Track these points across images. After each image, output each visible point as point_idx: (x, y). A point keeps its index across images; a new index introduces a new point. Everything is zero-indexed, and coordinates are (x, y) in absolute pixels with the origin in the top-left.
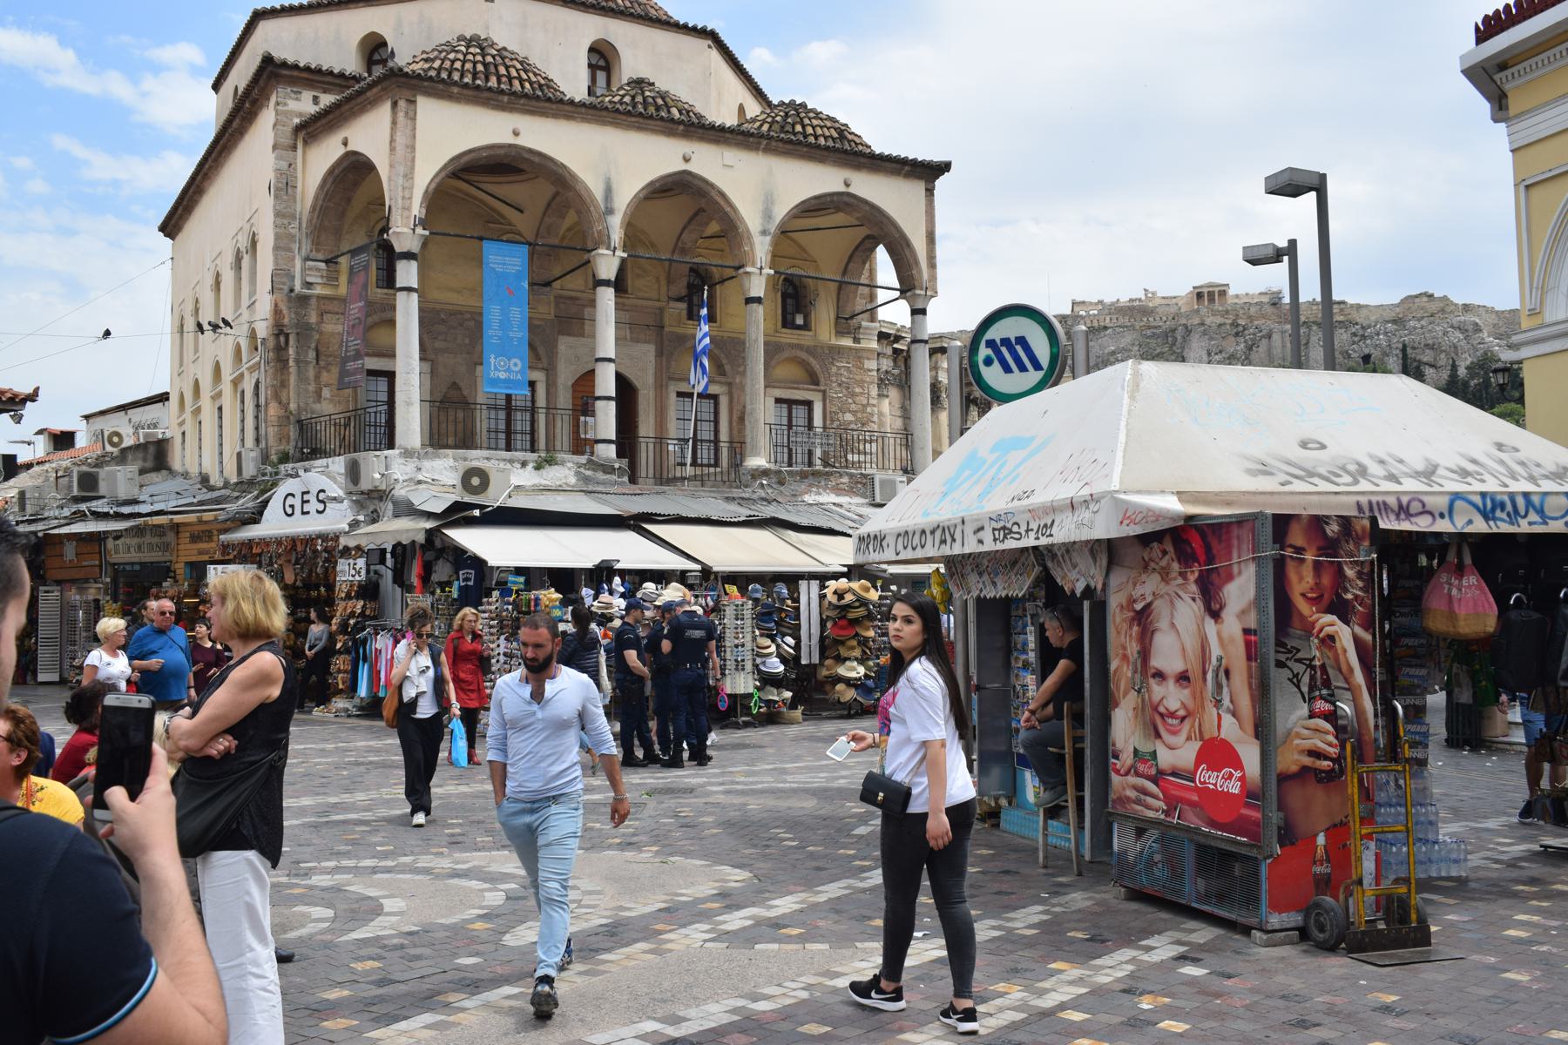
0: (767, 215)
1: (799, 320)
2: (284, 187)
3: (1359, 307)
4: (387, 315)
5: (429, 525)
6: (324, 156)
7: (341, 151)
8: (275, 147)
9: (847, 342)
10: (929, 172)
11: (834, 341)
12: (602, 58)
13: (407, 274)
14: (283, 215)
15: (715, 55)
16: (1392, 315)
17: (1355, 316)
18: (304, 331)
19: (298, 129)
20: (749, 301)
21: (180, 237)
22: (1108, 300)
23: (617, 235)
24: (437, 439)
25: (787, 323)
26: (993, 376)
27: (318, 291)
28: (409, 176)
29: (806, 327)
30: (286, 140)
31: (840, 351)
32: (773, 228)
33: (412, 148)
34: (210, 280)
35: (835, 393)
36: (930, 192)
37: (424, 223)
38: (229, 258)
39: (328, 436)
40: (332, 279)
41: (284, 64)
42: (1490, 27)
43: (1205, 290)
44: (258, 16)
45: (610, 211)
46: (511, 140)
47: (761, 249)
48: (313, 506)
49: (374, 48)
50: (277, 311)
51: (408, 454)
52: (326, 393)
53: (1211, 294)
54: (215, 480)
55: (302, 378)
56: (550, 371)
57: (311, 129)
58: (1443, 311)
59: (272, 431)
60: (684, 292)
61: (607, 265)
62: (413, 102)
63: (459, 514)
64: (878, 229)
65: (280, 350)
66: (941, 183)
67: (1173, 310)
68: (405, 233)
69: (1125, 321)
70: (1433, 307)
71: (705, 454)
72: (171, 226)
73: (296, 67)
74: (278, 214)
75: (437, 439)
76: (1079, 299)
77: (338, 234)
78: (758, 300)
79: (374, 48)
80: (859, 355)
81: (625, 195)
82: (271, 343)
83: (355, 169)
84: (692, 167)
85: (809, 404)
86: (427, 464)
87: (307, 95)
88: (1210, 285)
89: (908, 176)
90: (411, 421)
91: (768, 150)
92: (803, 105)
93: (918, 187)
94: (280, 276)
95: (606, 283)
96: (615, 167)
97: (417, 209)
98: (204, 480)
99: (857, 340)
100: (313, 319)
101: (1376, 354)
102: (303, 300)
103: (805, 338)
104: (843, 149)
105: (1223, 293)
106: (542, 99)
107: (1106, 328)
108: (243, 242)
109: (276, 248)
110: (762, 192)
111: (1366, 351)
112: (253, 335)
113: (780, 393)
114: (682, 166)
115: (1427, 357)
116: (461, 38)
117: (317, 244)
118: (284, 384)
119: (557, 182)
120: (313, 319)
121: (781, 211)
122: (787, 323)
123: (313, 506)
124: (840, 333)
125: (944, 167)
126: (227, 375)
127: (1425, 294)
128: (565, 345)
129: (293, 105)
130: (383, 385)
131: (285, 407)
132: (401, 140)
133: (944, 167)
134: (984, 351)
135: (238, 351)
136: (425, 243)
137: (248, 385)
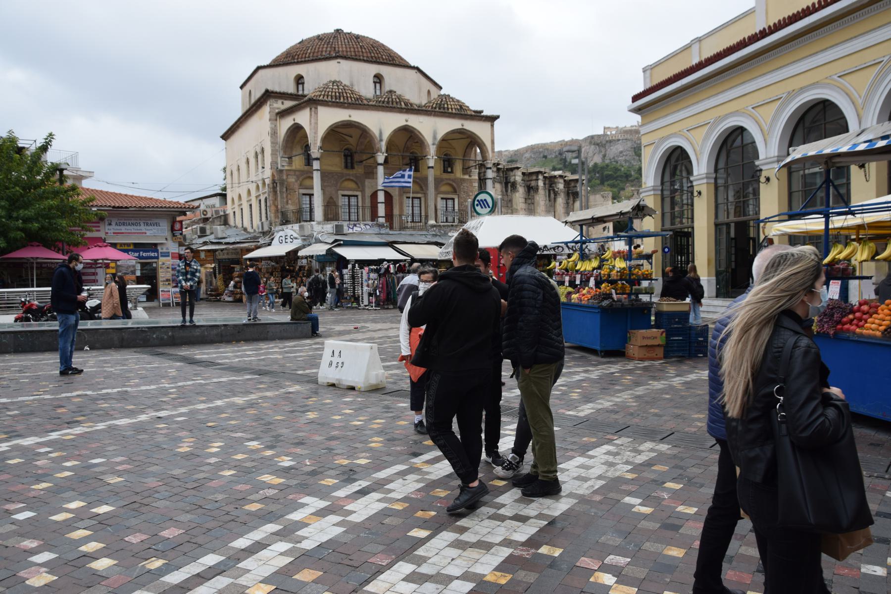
0: (435, 138)
1: (449, 170)
2: (274, 133)
4: (309, 175)
5: (328, 247)
6: (286, 124)
7: (293, 122)
8: (270, 120)
9: (467, 177)
10: (492, 119)
11: (462, 177)
12: (378, 79)
13: (316, 165)
14: (274, 143)
15: (419, 74)
18: (282, 183)
19: (278, 114)
20: (429, 167)
21: (229, 141)
22: (621, 126)
23: (384, 148)
24: (327, 218)
25: (445, 171)
26: (478, 209)
27: (286, 168)
28: (316, 133)
29: (452, 172)
30: (274, 117)
31: (464, 180)
32: (437, 142)
33: (316, 123)
34: (245, 160)
35: (463, 195)
36: (492, 126)
37: (321, 148)
38: (253, 154)
39: (291, 216)
40: (290, 163)
41: (272, 92)
42: (635, 98)
44: (259, 68)
45: (381, 140)
46: (346, 118)
47: (432, 150)
48: (289, 240)
49: (299, 80)
50: (273, 175)
51: (319, 223)
52: (290, 202)
54: (250, 229)
55: (282, 198)
56: (363, 191)
57: (283, 114)
59: (273, 215)
60: (408, 162)
61: (381, 158)
62: (316, 108)
63: (338, 243)
64: (473, 141)
65: (274, 188)
66: (496, 123)
68: (315, 152)
69: (628, 136)
71: (417, 219)
72: (226, 136)
73: (276, 93)
74: (272, 143)
75: (327, 218)
77: (292, 149)
78: (432, 167)
79: (299, 80)
80: (471, 181)
81: (386, 136)
82: (271, 186)
83: (297, 129)
84: (409, 123)
85: (453, 199)
86: (325, 226)
87: (280, 101)
89: (484, 121)
90: (319, 213)
91: (435, 115)
92: (449, 96)
93: (488, 125)
94: (274, 164)
95: (381, 164)
96: (383, 125)
97: (319, 144)
98: (245, 230)
99: (470, 176)
100: (285, 177)
102: (281, 171)
103: (452, 176)
104: (462, 112)
106: (359, 103)
107: (619, 140)
108: (259, 150)
109: (272, 154)
110: (432, 129)
112: (264, 183)
113: (442, 196)
114: (404, 123)
116: (330, 82)
117: (285, 152)
118: (276, 199)
119: (363, 131)
120: (285, 177)
121: (439, 136)
122: (445, 171)
123: (289, 240)
124: (464, 174)
125: (498, 117)
126: (254, 193)
128: (368, 182)
129: (275, 105)
130: (308, 198)
131: (277, 207)
132: (313, 121)
133: (498, 117)
134: (476, 203)
135: (258, 187)
136: (321, 156)
137: (263, 198)
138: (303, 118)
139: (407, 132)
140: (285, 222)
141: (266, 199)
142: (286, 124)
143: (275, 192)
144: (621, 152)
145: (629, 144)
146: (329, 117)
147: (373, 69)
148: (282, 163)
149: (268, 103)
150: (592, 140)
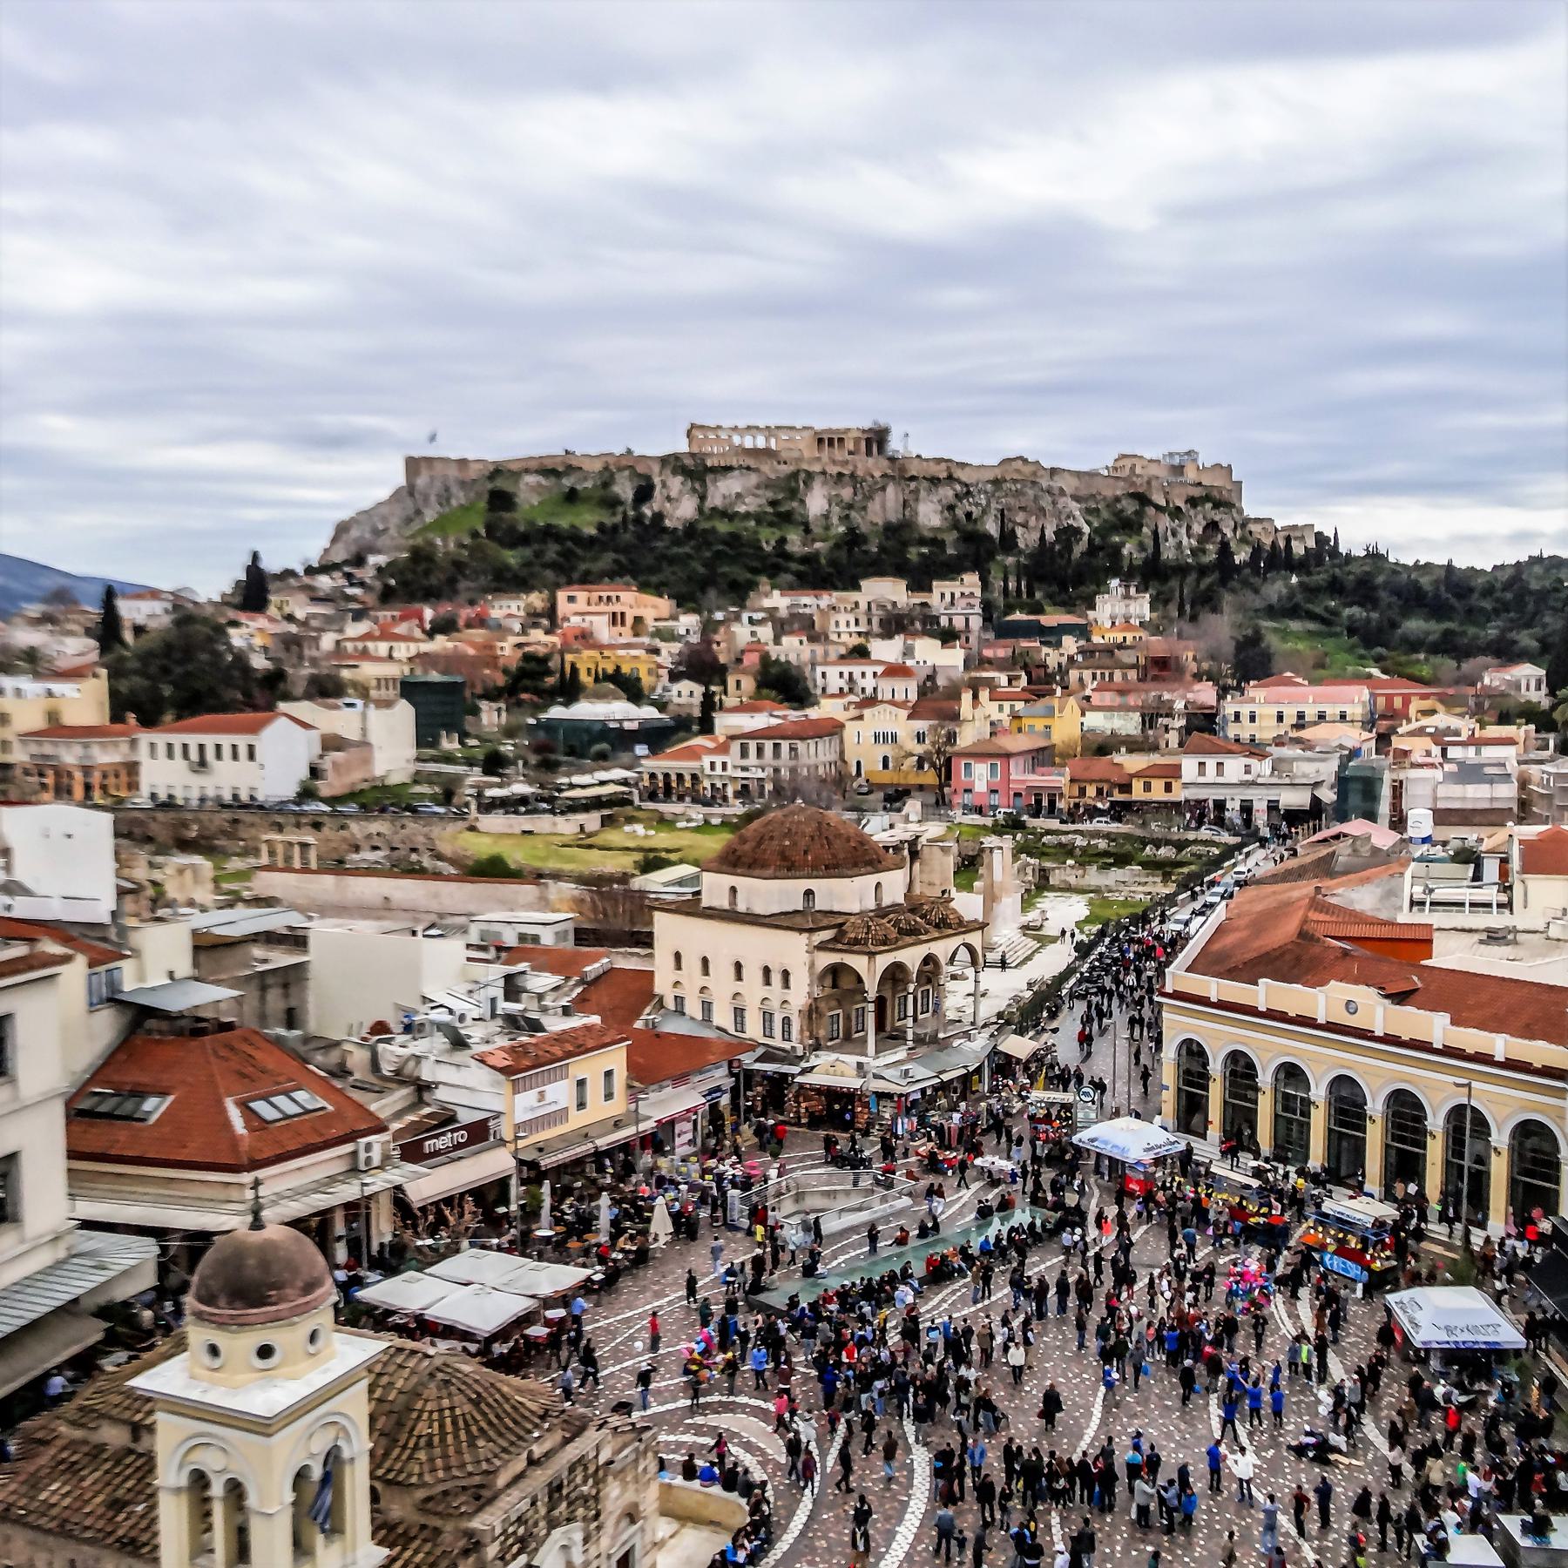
2: (812, 966)
3: (963, 465)
16: (990, 476)
17: (958, 473)
43: (826, 437)
49: (809, 894)
53: (831, 441)
58: (1034, 474)
67: (796, 454)
70: (1027, 470)
76: (698, 422)
79: (809, 894)
88: (830, 431)
101: (976, 512)
105: (841, 440)
111: (968, 508)
115: (1020, 518)
127: (1021, 458)
138: (858, 962)
139: (929, 959)
140: (817, 1047)
141: (786, 1021)
142: (826, 959)
143: (810, 1018)
144: (738, 495)
145: (753, 479)
146: (883, 961)
147: (873, 879)
148: (817, 992)
149: (805, 935)
150: (672, 463)
